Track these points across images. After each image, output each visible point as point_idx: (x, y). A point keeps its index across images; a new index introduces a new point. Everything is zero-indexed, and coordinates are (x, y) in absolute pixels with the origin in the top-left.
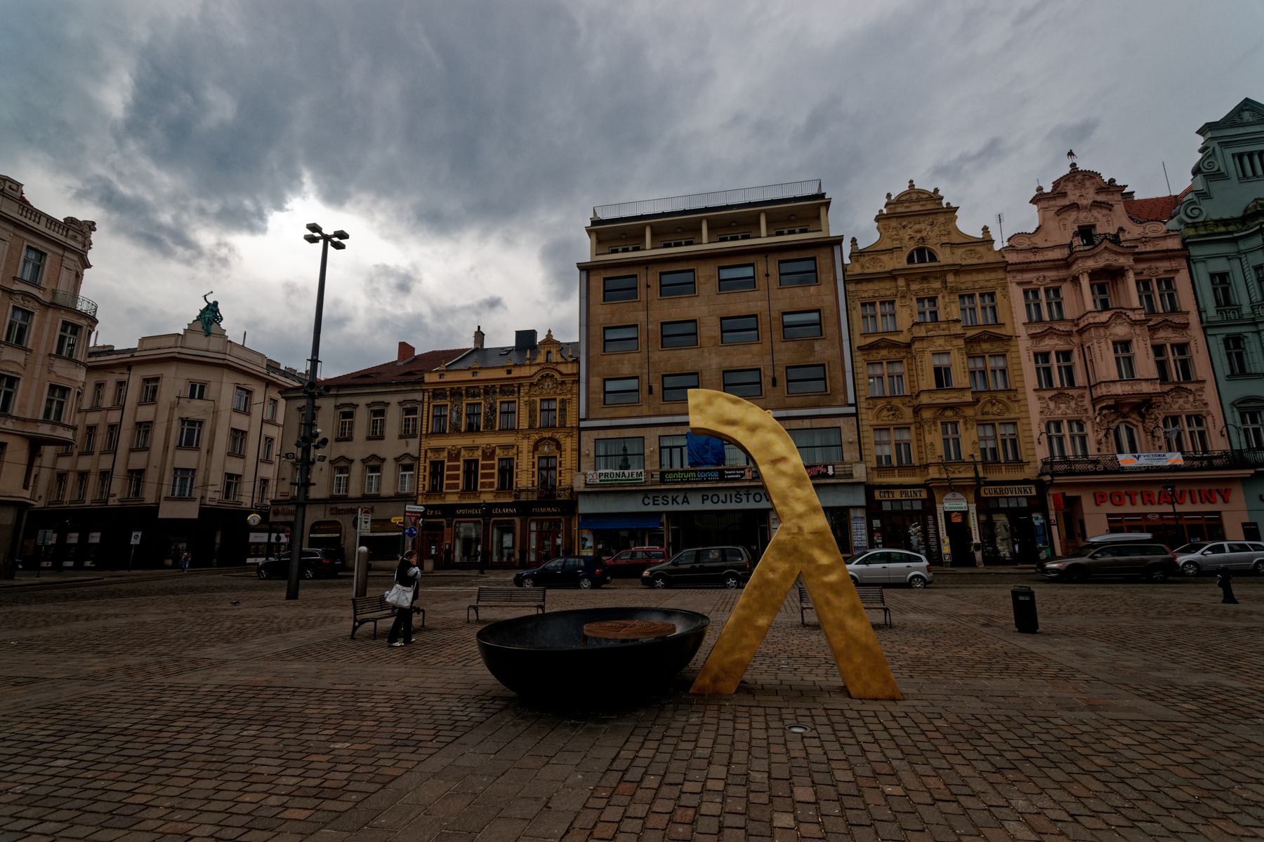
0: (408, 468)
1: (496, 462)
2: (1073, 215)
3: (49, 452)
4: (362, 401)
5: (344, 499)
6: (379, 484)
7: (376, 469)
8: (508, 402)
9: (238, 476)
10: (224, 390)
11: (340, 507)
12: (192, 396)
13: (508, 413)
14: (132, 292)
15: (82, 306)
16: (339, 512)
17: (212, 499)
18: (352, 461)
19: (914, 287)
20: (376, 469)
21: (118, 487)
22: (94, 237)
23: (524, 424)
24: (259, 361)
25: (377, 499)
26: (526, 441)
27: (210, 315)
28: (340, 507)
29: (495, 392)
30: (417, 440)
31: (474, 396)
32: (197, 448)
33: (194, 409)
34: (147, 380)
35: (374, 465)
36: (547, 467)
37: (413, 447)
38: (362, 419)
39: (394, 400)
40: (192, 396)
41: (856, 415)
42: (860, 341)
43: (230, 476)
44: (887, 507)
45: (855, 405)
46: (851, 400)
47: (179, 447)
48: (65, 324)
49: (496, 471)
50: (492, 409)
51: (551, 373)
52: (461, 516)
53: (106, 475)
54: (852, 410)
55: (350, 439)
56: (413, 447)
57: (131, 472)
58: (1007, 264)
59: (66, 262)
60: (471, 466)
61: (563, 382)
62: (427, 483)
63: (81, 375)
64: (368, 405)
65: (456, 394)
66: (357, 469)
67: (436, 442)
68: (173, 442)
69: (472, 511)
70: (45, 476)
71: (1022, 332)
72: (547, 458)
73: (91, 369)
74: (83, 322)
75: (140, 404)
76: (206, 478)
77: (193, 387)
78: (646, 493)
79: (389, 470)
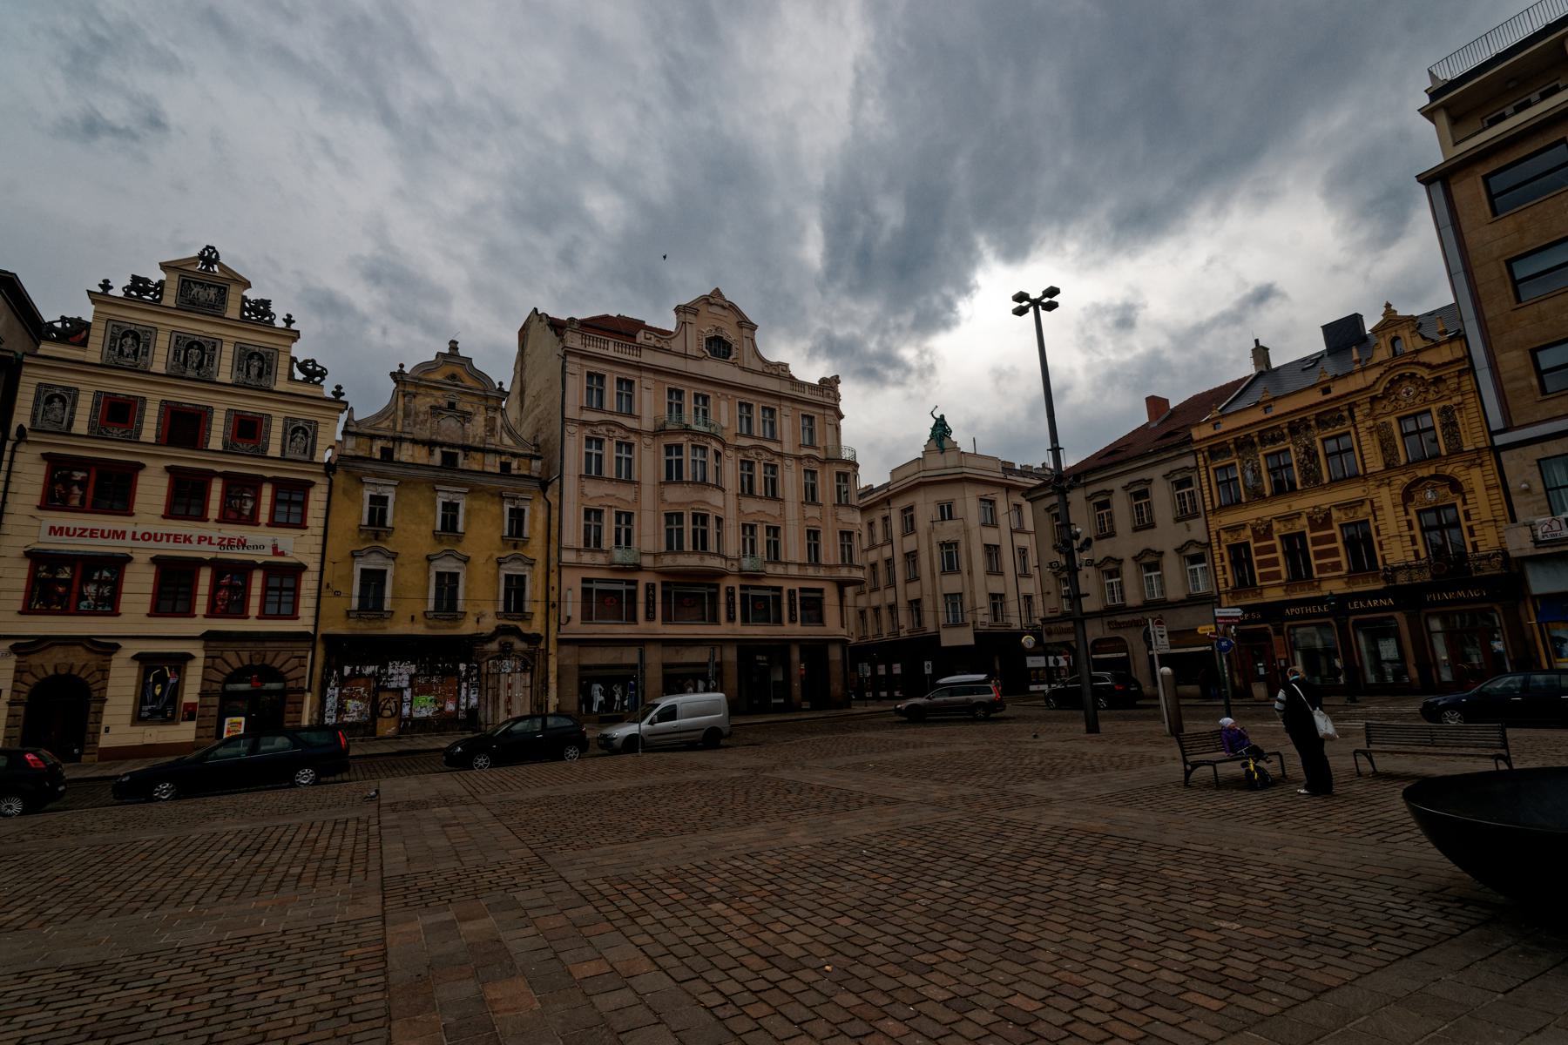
0: (1195, 559)
1: (1336, 530)
3: (849, 591)
4: (1117, 485)
5: (1122, 609)
6: (1162, 584)
7: (1154, 566)
8: (1337, 437)
9: (1002, 595)
10: (968, 503)
11: (1119, 619)
12: (943, 519)
13: (1340, 453)
14: (879, 429)
15: (846, 455)
16: (1119, 626)
17: (983, 623)
18: (1121, 561)
20: (1154, 566)
21: (903, 617)
22: (841, 388)
23: (1375, 463)
24: (992, 465)
25: (1164, 604)
26: (1385, 491)
27: (941, 429)
28: (1119, 619)
29: (1308, 427)
30: (1202, 520)
31: (1274, 441)
32: (959, 571)
33: (948, 531)
34: (904, 511)
35: (1150, 561)
36: (1439, 524)
37: (1197, 530)
38: (1121, 507)
39: (1156, 474)
40: (943, 519)
43: (993, 596)
47: (943, 572)
48: (838, 474)
49: (1339, 544)
50: (1311, 454)
51: (1407, 371)
52: (1294, 617)
53: (893, 608)
55: (1112, 534)
56: (1197, 530)
57: (910, 602)
59: (829, 419)
60: (1295, 545)
61: (1438, 380)
62: (1229, 576)
63: (857, 518)
64: (1125, 488)
65: (1245, 445)
66: (1129, 569)
67: (1230, 519)
68: (938, 569)
69: (1309, 610)
70: (851, 614)
72: (1436, 510)
73: (864, 510)
74: (849, 469)
75: (904, 535)
76: (973, 601)
77: (942, 508)
79: (1171, 564)
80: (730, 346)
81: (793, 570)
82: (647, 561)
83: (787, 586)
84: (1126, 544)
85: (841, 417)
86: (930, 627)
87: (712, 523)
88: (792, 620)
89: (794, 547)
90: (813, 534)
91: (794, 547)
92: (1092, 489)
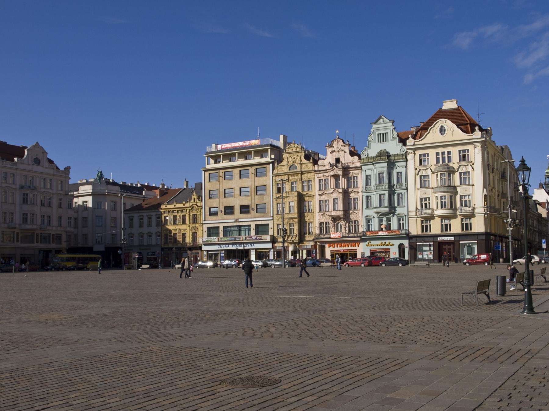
0: (159, 236)
2: (334, 153)
4: (145, 214)
7: (150, 236)
19: (291, 178)
20: (150, 236)
22: (71, 170)
35: (150, 235)
36: (194, 236)
38: (145, 220)
41: (273, 220)
42: (275, 197)
44: (278, 248)
45: (273, 217)
46: (272, 215)
54: (272, 218)
58: (315, 171)
71: (317, 193)
78: (218, 244)
79: (154, 236)
80: (40, 161)
81: (54, 228)
82: (17, 226)
83: (53, 233)
84: (145, 230)
85: (70, 179)
86: (90, 244)
87: (35, 215)
88: (53, 243)
89: (55, 222)
90: (60, 218)
91: (55, 222)
92: (139, 214)
